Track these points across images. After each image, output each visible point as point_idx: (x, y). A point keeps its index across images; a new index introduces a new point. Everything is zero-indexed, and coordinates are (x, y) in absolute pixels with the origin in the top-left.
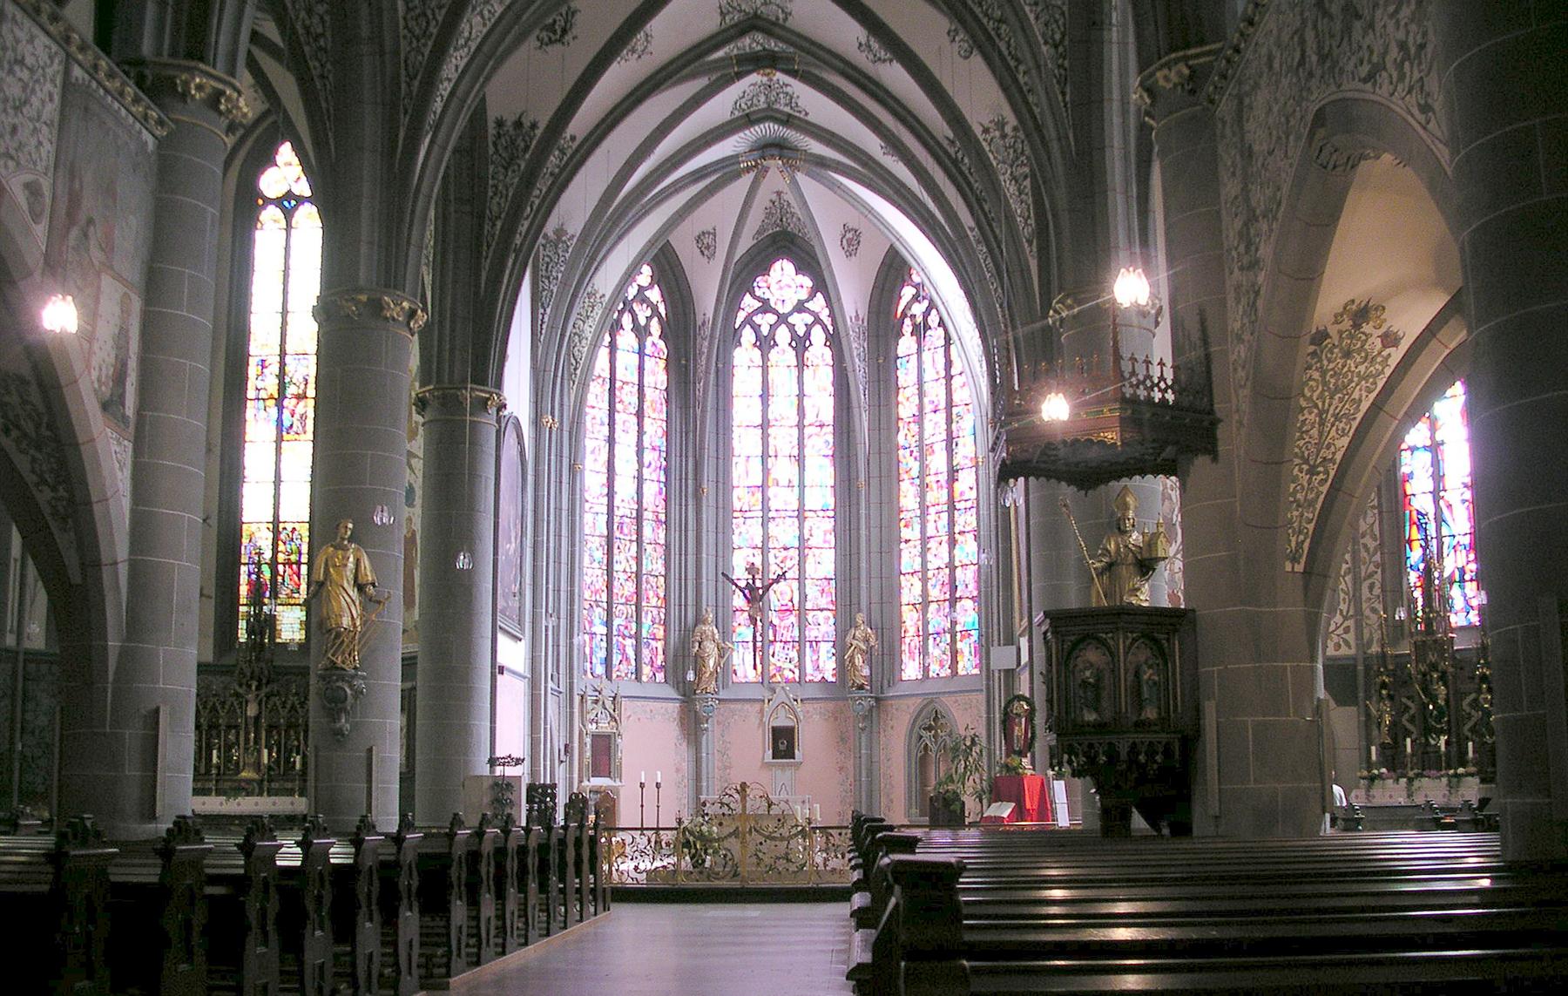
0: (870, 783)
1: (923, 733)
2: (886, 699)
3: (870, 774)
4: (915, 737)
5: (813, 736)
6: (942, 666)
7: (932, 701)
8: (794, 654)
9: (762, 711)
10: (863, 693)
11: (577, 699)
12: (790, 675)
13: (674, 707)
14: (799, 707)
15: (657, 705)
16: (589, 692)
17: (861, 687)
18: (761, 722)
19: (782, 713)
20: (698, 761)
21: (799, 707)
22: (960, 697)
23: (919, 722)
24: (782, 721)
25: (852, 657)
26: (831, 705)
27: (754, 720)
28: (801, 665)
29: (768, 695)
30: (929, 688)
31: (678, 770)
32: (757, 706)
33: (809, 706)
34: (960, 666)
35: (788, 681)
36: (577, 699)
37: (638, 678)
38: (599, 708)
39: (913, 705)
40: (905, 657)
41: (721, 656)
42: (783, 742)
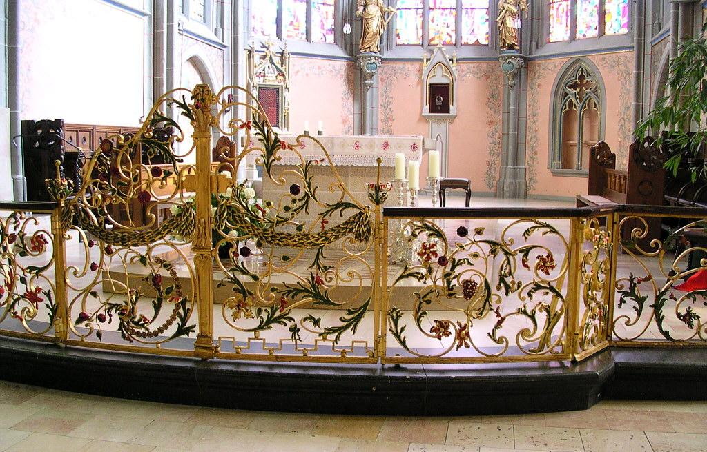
0: (517, 137)
1: (569, 90)
2: (534, 59)
3: (517, 128)
4: (560, 93)
5: (466, 94)
6: (589, 27)
7: (578, 60)
8: (451, 20)
9: (420, 70)
10: (512, 53)
11: (243, 56)
12: (448, 40)
13: (341, 66)
14: (454, 67)
15: (332, 62)
16: (257, 47)
17: (511, 47)
18: (420, 81)
19: (439, 71)
20: (363, 114)
21: (454, 67)
22: (607, 55)
23: (565, 80)
24: (439, 79)
25: (503, 19)
26: (484, 65)
27: (413, 78)
28: (457, 30)
29: (426, 55)
30: (574, 48)
31: (344, 122)
32: (417, 66)
33: (463, 66)
34: (607, 26)
35: (445, 44)
36: (243, 56)
37: (308, 38)
38: (267, 62)
39: (559, 64)
40: (553, 21)
41: (383, 19)
42: (440, 98)
